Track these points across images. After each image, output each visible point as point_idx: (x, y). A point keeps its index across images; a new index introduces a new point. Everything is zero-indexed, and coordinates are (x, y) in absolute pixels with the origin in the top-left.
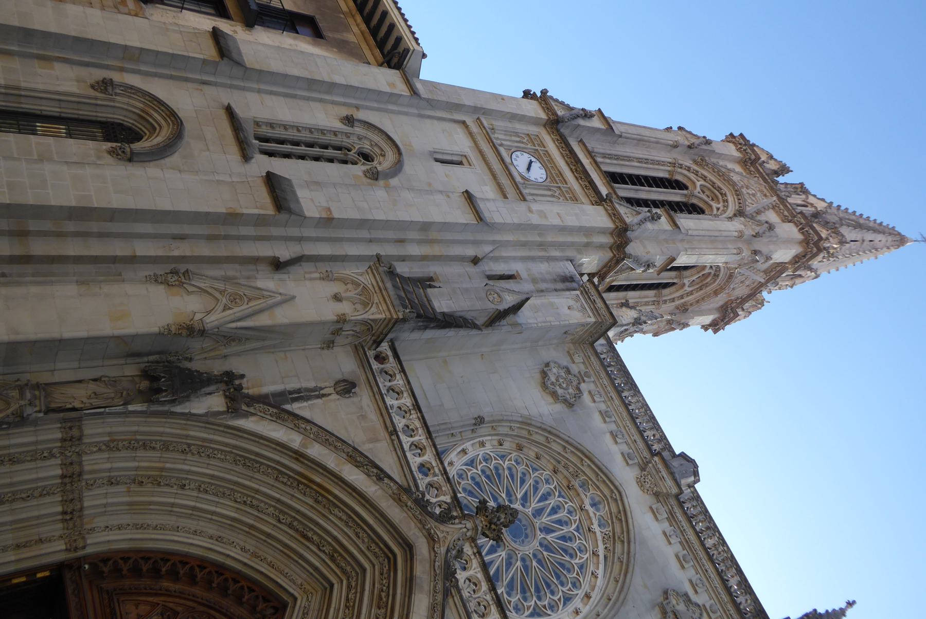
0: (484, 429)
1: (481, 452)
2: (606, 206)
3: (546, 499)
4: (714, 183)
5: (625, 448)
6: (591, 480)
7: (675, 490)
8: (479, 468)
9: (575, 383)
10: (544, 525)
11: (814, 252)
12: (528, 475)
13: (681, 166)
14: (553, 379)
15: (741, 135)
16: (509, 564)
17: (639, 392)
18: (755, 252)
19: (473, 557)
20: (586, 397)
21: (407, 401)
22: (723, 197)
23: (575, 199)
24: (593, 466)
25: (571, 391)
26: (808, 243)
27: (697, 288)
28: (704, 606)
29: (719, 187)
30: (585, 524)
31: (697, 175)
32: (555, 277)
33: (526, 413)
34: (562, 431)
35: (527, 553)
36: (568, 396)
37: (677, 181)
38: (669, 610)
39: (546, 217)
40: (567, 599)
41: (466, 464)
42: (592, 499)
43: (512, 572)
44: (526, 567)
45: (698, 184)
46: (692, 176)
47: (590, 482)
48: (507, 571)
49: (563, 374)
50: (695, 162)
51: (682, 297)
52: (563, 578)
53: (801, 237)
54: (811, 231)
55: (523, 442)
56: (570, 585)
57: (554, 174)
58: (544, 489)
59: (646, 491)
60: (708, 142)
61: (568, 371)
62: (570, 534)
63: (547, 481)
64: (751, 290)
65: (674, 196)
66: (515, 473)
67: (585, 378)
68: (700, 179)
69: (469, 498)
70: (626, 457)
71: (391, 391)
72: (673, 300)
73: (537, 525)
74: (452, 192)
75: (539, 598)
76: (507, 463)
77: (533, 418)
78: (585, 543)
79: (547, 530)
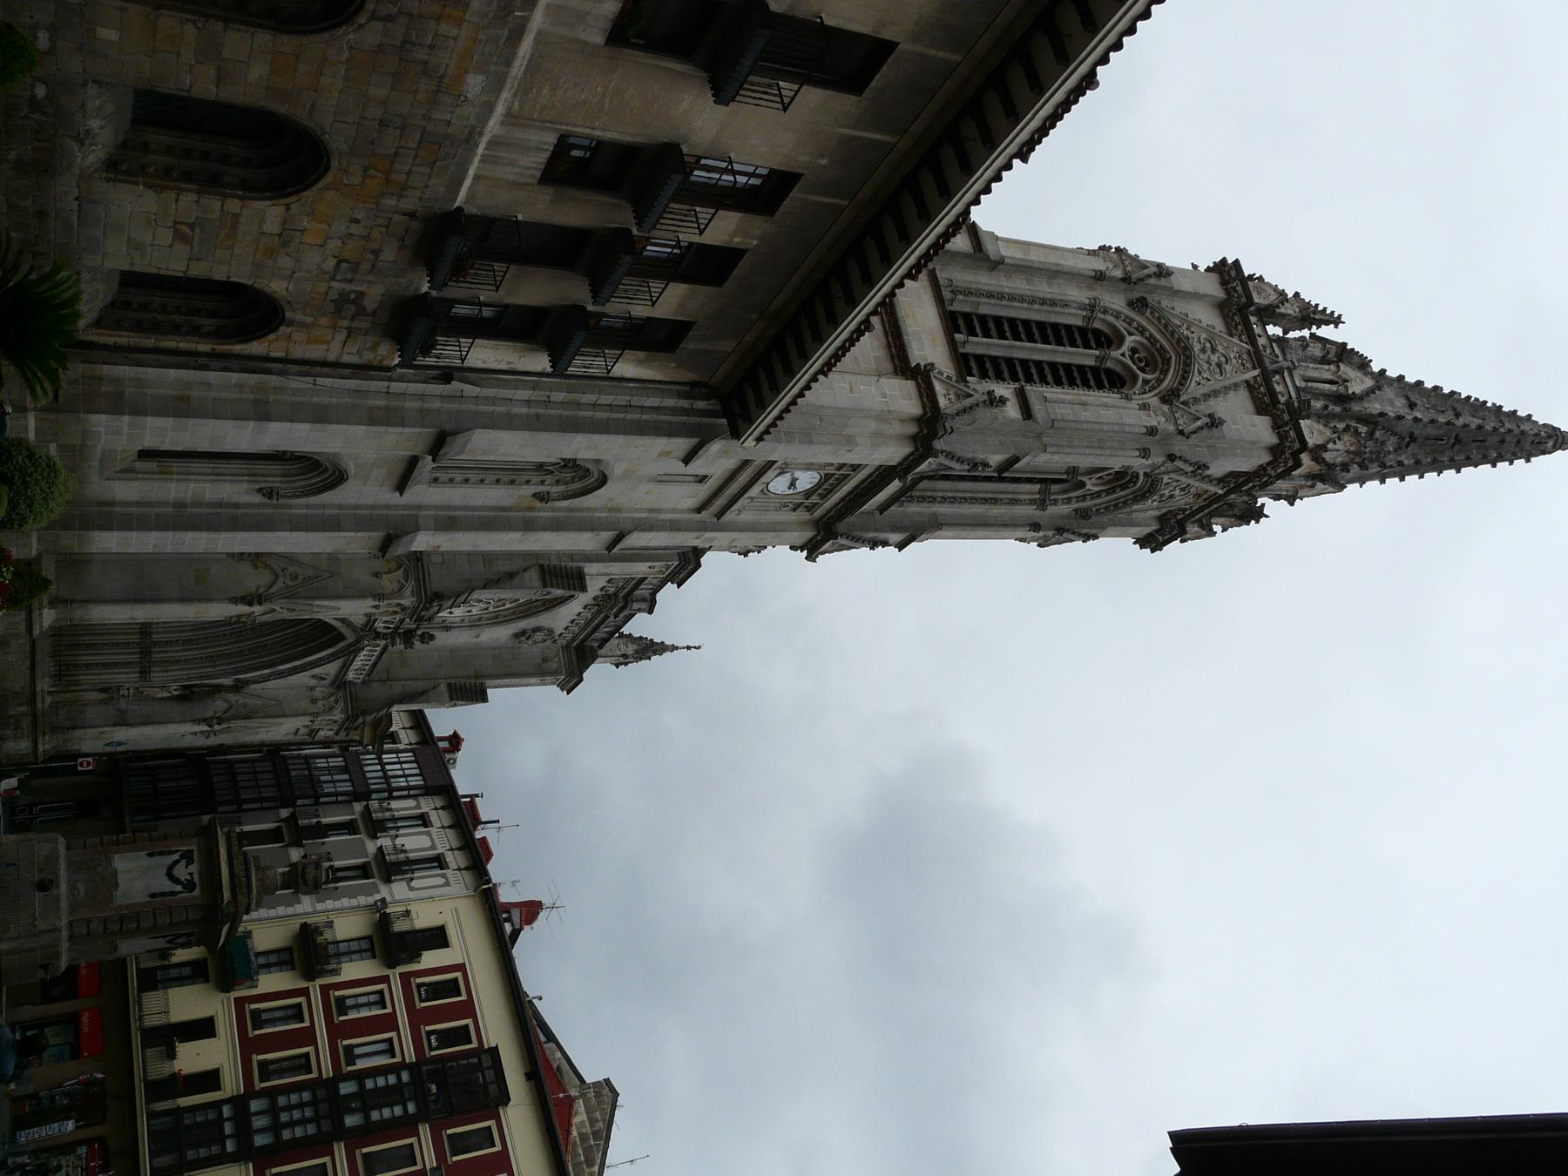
2: (920, 381)
4: (1156, 341)
11: (1289, 465)
13: (1105, 312)
15: (1237, 263)
18: (1171, 457)
22: (1163, 364)
26: (1283, 452)
27: (1110, 489)
31: (1130, 324)
37: (1097, 333)
45: (1130, 341)
46: (1120, 325)
50: (1131, 304)
51: (1084, 498)
53: (1272, 439)
54: (1292, 433)
60: (1162, 271)
64: (1205, 500)
68: (1134, 331)
72: (1069, 500)
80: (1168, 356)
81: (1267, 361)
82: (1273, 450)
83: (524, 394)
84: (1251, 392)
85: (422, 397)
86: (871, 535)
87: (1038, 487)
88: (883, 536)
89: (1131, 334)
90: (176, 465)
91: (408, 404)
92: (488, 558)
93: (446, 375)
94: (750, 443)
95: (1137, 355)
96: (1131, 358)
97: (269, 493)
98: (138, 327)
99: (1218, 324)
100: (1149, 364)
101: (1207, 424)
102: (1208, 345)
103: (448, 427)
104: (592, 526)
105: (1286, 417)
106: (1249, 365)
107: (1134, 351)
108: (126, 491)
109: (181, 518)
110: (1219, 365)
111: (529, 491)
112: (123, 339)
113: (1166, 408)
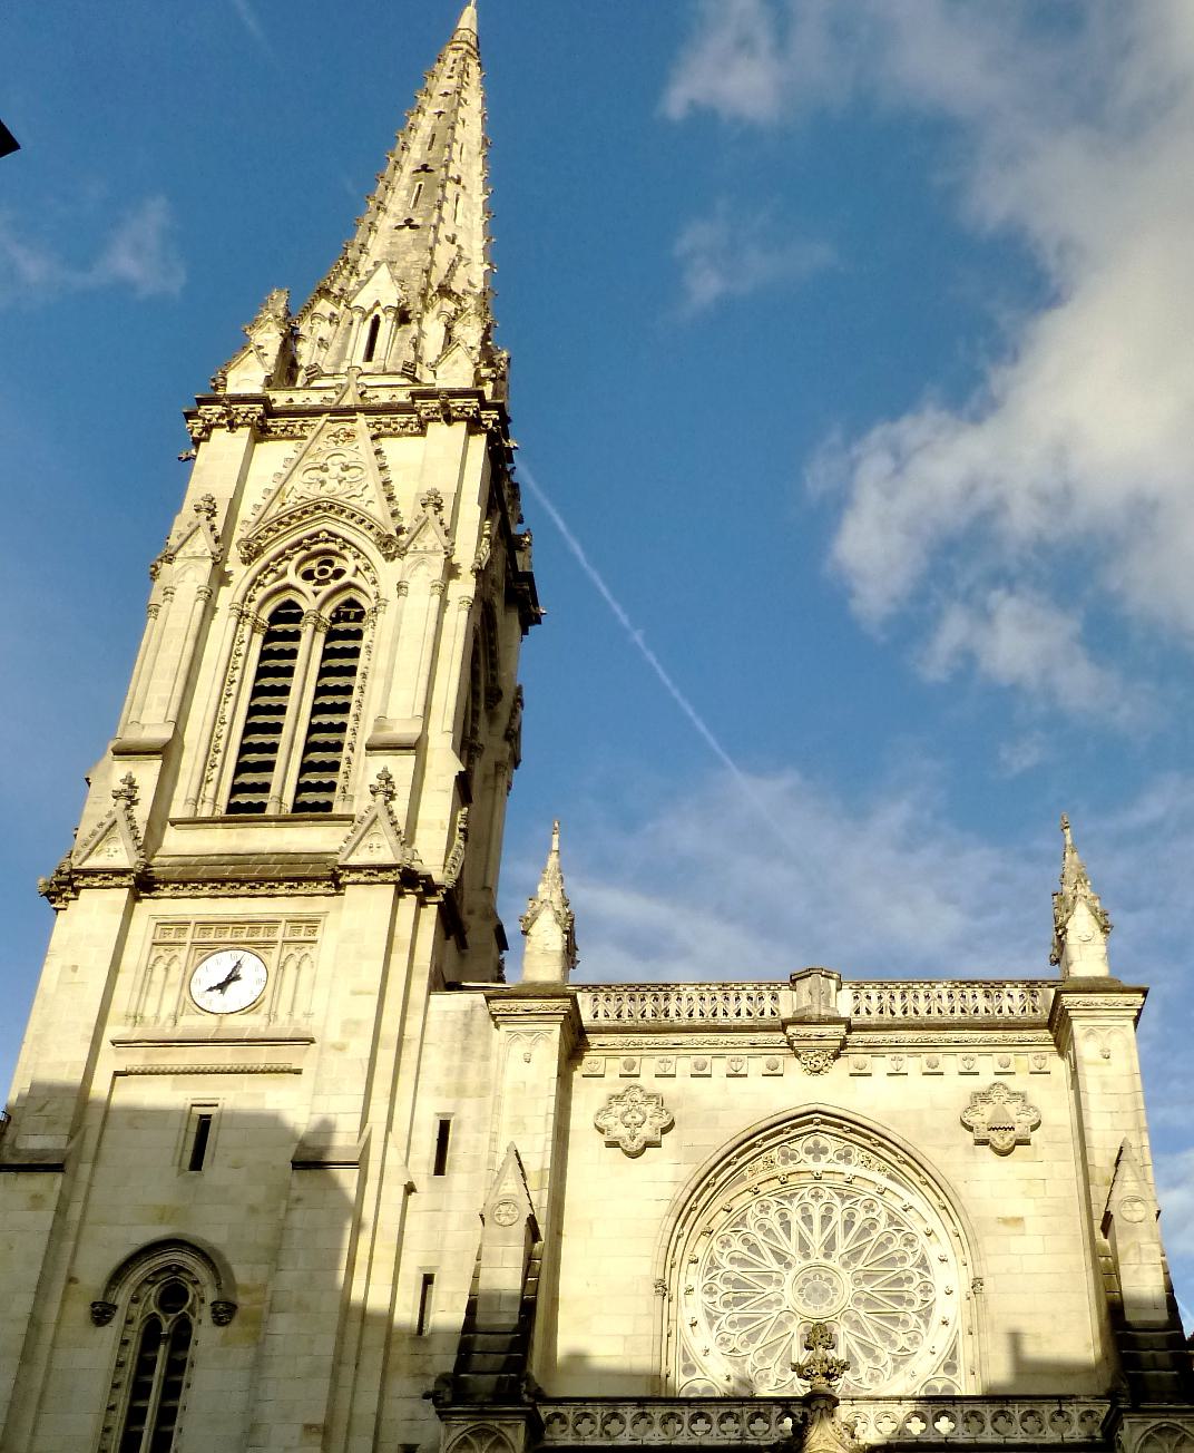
0: (677, 1287)
1: (699, 1297)
2: (348, 880)
3: (789, 1222)
5: (757, 1066)
6: (782, 1142)
7: (842, 1029)
8: (722, 1310)
9: (639, 1097)
10: (823, 1248)
12: (750, 1237)
13: (248, 599)
14: (620, 1132)
16: (857, 1325)
17: (678, 985)
19: (855, 1409)
20: (662, 1086)
21: (629, 1412)
23: (312, 923)
24: (767, 1132)
25: (650, 1109)
28: (997, 1074)
29: (310, 538)
30: (839, 1181)
32: (458, 1045)
33: (665, 1206)
34: (706, 1159)
35: (852, 1293)
36: (656, 1120)
38: (984, 1134)
39: (358, 1023)
40: (923, 1264)
41: (711, 1324)
42: (808, 1151)
43: (870, 1327)
44: (870, 1302)
45: (293, 578)
46: (271, 582)
47: (785, 1144)
48: (865, 1334)
49: (619, 1109)
52: (897, 1255)
55: (701, 1224)
56: (909, 1250)
57: (255, 936)
58: (773, 1221)
59: (825, 1068)
61: (618, 1098)
62: (845, 1213)
63: (765, 1209)
65: (310, 650)
66: (740, 1256)
67: (633, 1072)
68: (280, 568)
69: (758, 1344)
70: (773, 1073)
71: (607, 1428)
73: (823, 1261)
74: (290, 1188)
75: (911, 1302)
76: (724, 1262)
77: (676, 1197)
78: (862, 1198)
79: (830, 1245)
80: (326, 535)
81: (348, 401)
82: (471, 432)
84: (391, 435)
89: (284, 573)
95: (316, 574)
96: (319, 583)
99: (285, 449)
100: (326, 557)
101: (436, 512)
102: (313, 473)
105: (435, 403)
106: (348, 426)
107: (308, 575)
110: (346, 468)
113: (408, 559)
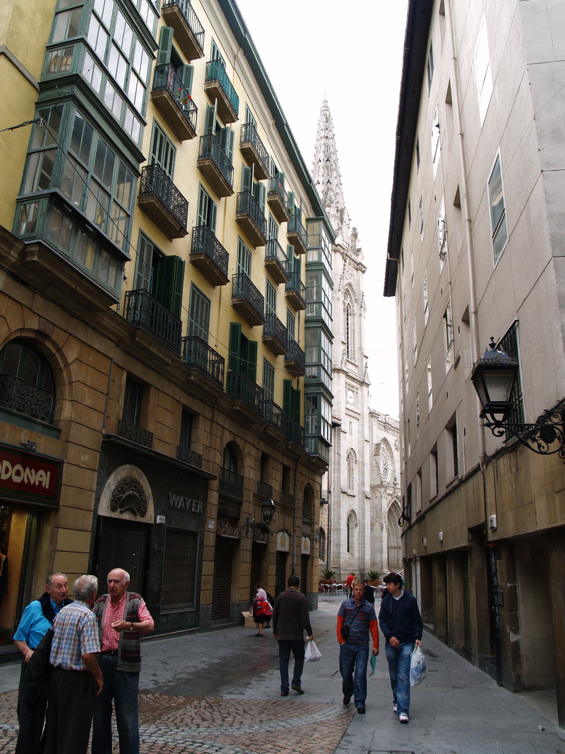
83: (333, 474)
85: (334, 497)
86: (364, 369)
87: (349, 317)
88: (364, 365)
90: (350, 545)
91: (336, 500)
92: (371, 473)
93: (329, 492)
94: (340, 422)
97: (356, 525)
98: (323, 553)
103: (341, 491)
104: (363, 448)
108: (356, 555)
109: (362, 543)
111: (354, 465)
112: (326, 556)
